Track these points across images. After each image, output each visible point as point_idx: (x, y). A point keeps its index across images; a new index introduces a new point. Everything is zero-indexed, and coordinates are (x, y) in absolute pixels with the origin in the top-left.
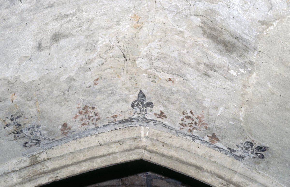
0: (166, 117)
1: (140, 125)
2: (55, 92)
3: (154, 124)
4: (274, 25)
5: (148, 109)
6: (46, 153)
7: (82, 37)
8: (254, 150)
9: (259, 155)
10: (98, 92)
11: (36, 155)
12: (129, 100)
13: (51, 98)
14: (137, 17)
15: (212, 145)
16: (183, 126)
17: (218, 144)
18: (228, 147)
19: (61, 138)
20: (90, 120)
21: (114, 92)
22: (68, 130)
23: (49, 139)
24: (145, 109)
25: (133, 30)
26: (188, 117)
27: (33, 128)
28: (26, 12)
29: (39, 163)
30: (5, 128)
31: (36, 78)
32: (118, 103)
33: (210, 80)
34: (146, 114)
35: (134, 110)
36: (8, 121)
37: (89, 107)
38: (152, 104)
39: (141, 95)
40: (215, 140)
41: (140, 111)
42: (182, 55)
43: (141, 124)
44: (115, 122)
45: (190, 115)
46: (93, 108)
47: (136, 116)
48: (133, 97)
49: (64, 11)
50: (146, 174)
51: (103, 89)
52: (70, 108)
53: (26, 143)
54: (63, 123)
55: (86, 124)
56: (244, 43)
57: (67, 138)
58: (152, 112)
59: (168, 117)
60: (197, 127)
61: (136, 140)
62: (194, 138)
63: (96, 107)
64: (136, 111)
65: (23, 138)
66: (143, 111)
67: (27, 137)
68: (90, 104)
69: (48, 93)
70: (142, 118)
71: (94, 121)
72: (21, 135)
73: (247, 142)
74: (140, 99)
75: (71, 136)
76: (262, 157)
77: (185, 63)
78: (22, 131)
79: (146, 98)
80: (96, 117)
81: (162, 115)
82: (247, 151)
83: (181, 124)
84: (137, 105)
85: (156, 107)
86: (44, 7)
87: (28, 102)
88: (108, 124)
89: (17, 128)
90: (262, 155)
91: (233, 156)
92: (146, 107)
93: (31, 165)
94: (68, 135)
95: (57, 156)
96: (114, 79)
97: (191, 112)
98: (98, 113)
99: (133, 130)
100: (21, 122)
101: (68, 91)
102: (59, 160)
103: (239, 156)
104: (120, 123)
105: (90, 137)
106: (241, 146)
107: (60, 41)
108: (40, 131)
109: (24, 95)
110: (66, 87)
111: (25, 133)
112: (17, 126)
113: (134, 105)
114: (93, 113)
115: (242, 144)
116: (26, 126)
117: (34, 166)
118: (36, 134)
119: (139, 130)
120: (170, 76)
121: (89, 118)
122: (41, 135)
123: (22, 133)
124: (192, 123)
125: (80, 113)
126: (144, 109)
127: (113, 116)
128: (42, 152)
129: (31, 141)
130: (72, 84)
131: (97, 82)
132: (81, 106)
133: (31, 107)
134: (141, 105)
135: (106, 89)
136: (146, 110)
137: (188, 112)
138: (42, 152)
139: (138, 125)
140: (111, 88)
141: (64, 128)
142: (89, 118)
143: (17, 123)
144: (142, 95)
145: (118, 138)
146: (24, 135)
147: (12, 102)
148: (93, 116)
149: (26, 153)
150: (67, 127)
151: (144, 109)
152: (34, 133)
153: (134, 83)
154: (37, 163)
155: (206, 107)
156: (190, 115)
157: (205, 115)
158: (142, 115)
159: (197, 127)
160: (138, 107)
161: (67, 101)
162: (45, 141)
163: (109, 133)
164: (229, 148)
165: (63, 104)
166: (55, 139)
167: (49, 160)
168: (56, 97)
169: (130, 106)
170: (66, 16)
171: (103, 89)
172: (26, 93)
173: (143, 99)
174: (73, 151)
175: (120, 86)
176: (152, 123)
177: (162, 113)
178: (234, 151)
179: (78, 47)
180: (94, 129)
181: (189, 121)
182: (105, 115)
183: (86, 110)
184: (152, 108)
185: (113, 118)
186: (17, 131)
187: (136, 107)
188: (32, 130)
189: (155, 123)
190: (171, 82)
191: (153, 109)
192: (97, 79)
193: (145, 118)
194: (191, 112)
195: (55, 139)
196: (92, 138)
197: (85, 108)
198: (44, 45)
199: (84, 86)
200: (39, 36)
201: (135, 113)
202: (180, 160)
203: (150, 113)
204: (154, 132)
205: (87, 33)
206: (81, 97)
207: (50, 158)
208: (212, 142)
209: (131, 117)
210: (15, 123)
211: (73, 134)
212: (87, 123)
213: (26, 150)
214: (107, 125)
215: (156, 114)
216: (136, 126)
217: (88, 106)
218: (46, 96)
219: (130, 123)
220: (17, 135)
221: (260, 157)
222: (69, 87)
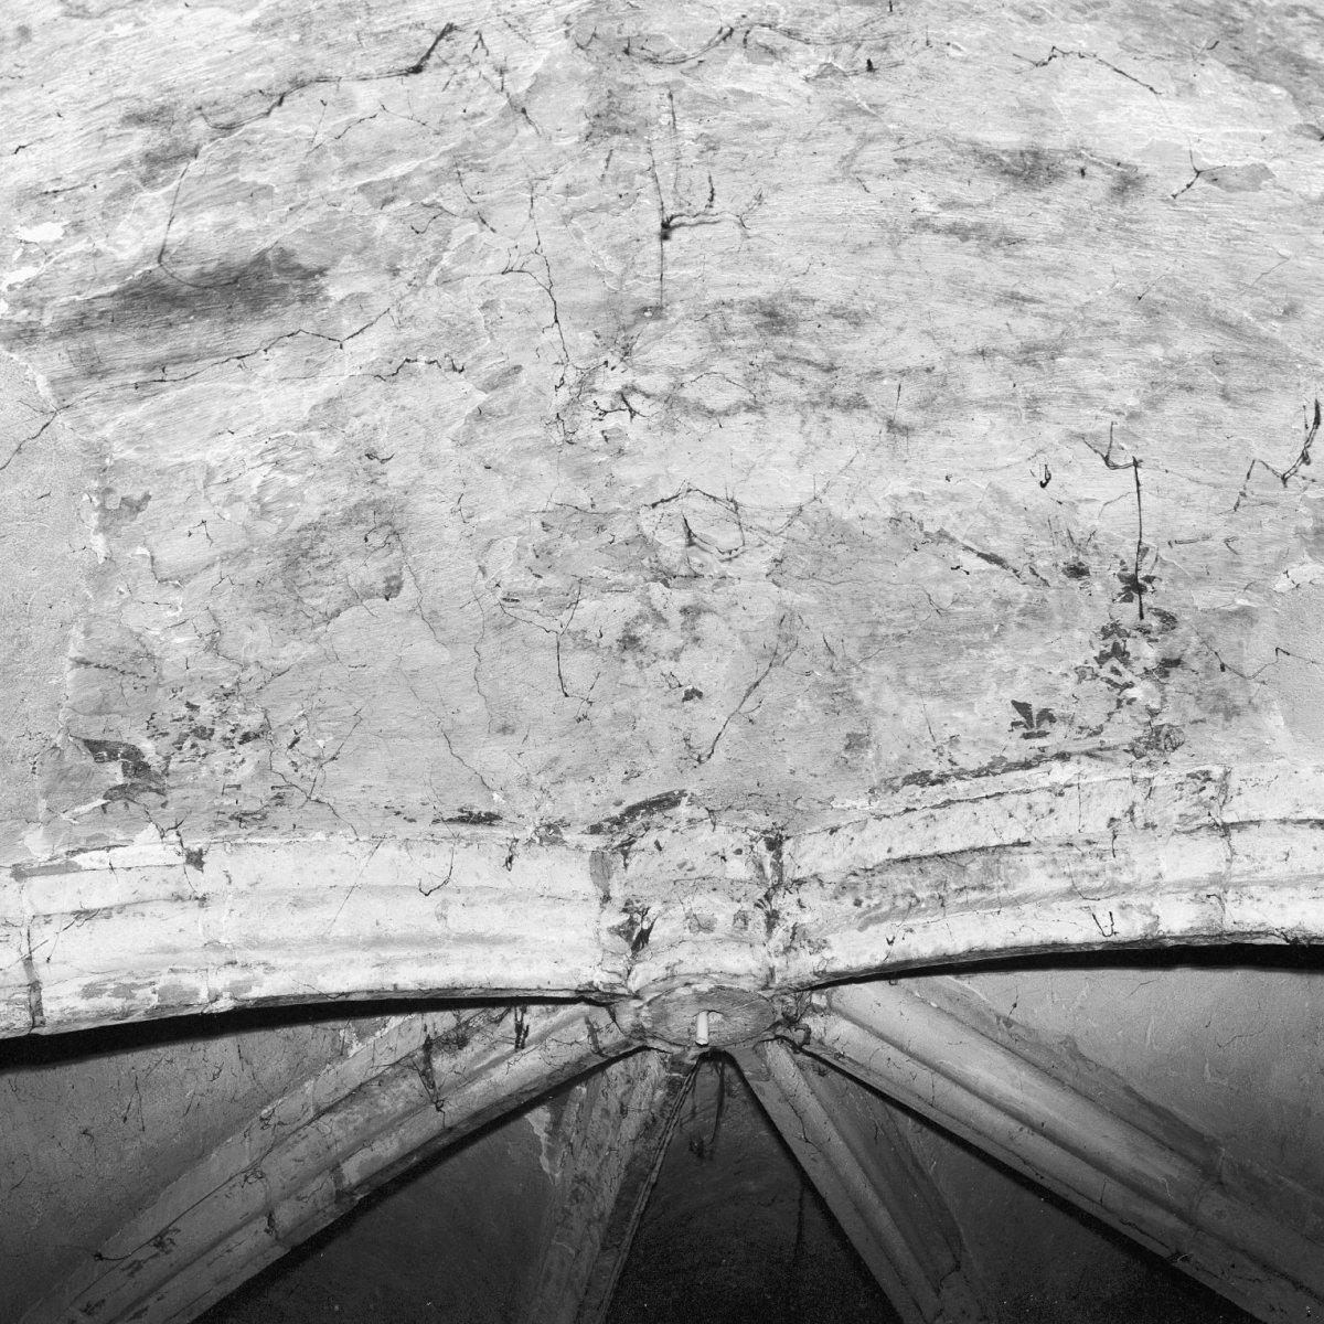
4: (96, 533)
14: (616, 180)
28: (1122, 330)
49: (963, 259)
86: (1042, 309)
170: (959, 232)
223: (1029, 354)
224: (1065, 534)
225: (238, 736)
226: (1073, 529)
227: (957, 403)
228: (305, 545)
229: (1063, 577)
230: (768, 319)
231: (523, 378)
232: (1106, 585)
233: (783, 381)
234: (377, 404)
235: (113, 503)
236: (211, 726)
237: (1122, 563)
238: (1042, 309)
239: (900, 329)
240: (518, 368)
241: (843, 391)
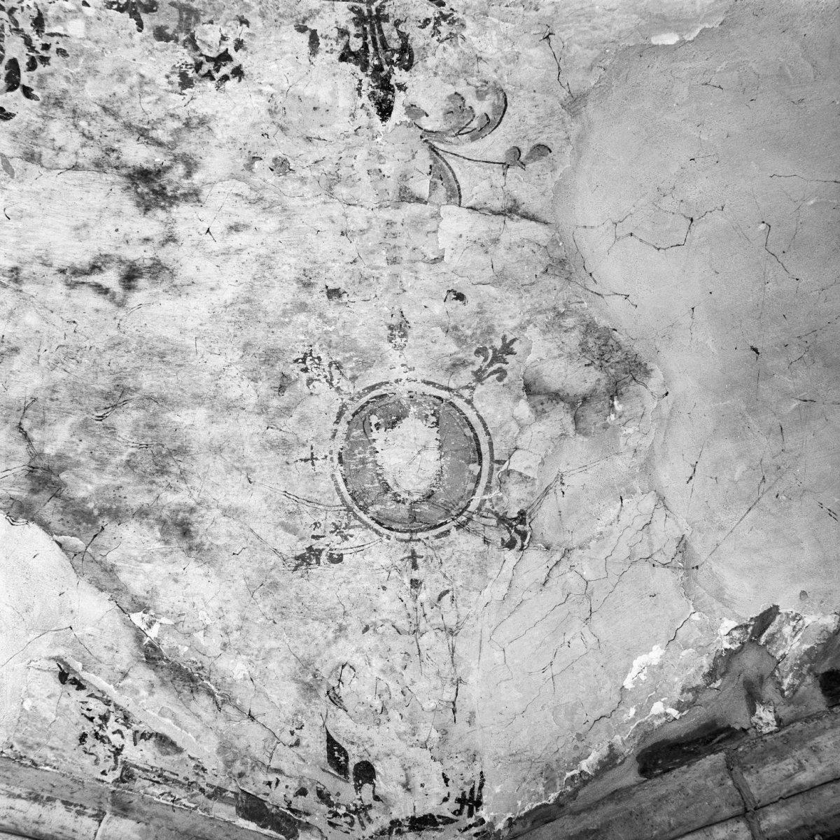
50: (475, 825)
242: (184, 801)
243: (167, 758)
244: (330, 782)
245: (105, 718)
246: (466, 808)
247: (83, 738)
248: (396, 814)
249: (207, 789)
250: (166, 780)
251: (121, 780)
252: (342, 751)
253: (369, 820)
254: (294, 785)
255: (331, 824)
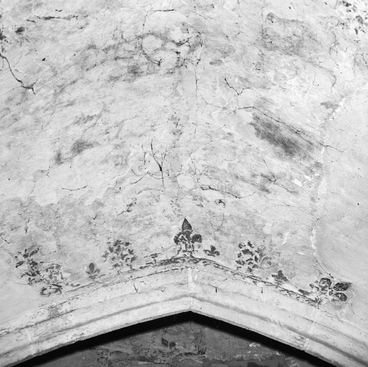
0: (218, 254)
1: (187, 267)
2: (78, 221)
3: (204, 264)
4: (341, 106)
5: (196, 244)
6: (69, 303)
7: (110, 148)
8: (333, 289)
9: (340, 295)
10: (133, 222)
11: (56, 306)
12: (171, 233)
13: (74, 228)
14: (176, 118)
15: (279, 289)
16: (240, 264)
17: (286, 286)
18: (299, 288)
19: (88, 284)
20: (123, 259)
21: (152, 222)
22: (97, 273)
23: (72, 285)
24: (191, 244)
25: (172, 137)
26: (246, 252)
27: (53, 268)
28: (42, 111)
29: (59, 315)
30: (17, 267)
31: (55, 201)
32: (157, 237)
33: (269, 196)
34: (193, 251)
35: (179, 246)
36: (21, 258)
37: (122, 242)
38: (201, 236)
39: (186, 226)
40: (283, 281)
41: (186, 247)
42: (233, 166)
43: (188, 265)
44: (155, 263)
45: (248, 247)
46: (127, 244)
47: (181, 254)
48: (176, 228)
49: (87, 112)
50: (203, 357)
51: (139, 219)
52: (98, 242)
53: (44, 289)
54: (89, 263)
55: (119, 266)
56: (307, 138)
57: (95, 284)
58: (201, 248)
59: (221, 254)
60: (258, 264)
61: (183, 286)
62: (256, 280)
63: (130, 242)
64: (181, 248)
65: (39, 282)
66: (190, 247)
67: (45, 280)
68: (122, 238)
69: (69, 222)
70: (188, 257)
71: (129, 262)
72: (37, 277)
73: (323, 279)
74: (185, 231)
75: (100, 281)
76: (344, 298)
77: (237, 177)
78: (38, 272)
79: (192, 229)
80: (131, 256)
81: (213, 251)
82: (324, 292)
83: (237, 262)
84: (181, 240)
85: (206, 241)
86: (63, 105)
87: (45, 233)
88: (146, 265)
89: (32, 267)
90: (344, 295)
91: (306, 301)
92: (193, 242)
93: (50, 319)
94: (96, 280)
95: (83, 306)
96: (152, 204)
97: (249, 244)
98: (133, 251)
99: (178, 273)
100: (37, 259)
101: (94, 219)
102: (85, 312)
103: (314, 299)
104: (162, 264)
105: (124, 283)
106: (316, 285)
107: (84, 152)
108: (61, 273)
109: (40, 223)
110: (92, 214)
111: (42, 276)
112: (32, 265)
113: (178, 239)
114: (127, 250)
115: (317, 282)
116: (44, 265)
117: (53, 320)
118: (55, 277)
119: (185, 273)
120: (221, 197)
121: (123, 257)
122: (62, 278)
123: (38, 275)
124: (251, 259)
125: (111, 250)
126: (191, 245)
127: (152, 255)
128: (65, 302)
129: (51, 287)
130: (99, 210)
131: (131, 208)
132: (112, 241)
133: (49, 239)
134: (186, 239)
135: (142, 218)
136: (193, 246)
137: (246, 244)
138: (65, 302)
139: (184, 267)
140: (148, 217)
141: (91, 270)
142: (122, 257)
143: (32, 260)
144: (187, 225)
145: (159, 284)
146: (41, 278)
147: (25, 232)
148: (127, 255)
149: (44, 304)
150: (95, 269)
151: (191, 245)
152: (53, 275)
153: (177, 209)
154: (58, 315)
155: (267, 235)
156: (248, 247)
157: (267, 246)
158: (188, 253)
159: (258, 264)
160: (183, 242)
161: (94, 234)
162: (67, 287)
163: (148, 278)
164: (300, 291)
165: (90, 237)
166: (80, 285)
167: (73, 312)
168: (81, 227)
169: (173, 241)
170: (90, 118)
171: (139, 219)
172: (43, 220)
173: (189, 230)
174: (102, 300)
175: (159, 213)
176: (201, 263)
177: (213, 248)
178: (308, 293)
179: (106, 161)
180: (128, 272)
181: (248, 256)
182: (142, 254)
183: (118, 247)
184: (200, 243)
185: (152, 257)
186: (32, 272)
187: (181, 243)
188: (50, 271)
189: (206, 264)
190: (222, 204)
191: (202, 243)
192: (131, 205)
193: (193, 257)
194: (249, 244)
195: (80, 285)
196: (126, 284)
197: (117, 243)
198: (64, 156)
199: (114, 213)
200: (58, 144)
201: (179, 251)
202: (239, 310)
203: (199, 250)
204: (204, 275)
205: (116, 142)
206: (111, 229)
207: (73, 309)
208: (278, 284)
209: (175, 256)
210: (29, 261)
211: (102, 278)
212: (120, 264)
213: (44, 299)
214: (145, 267)
215: (205, 251)
216: (181, 268)
217: (121, 241)
218: (68, 226)
219: (174, 264)
220: (32, 278)
221: (341, 299)
222: (96, 214)
223: (62, 89)
224: (29, 40)
225: (350, 8)
226: (28, 43)
227: (77, 63)
228: (291, 49)
229: (24, 26)
230: (136, 71)
231: (210, 60)
232: (8, 32)
233: (130, 49)
234: (253, 76)
235: (329, 111)
236: (356, 18)
237: (7, 42)
238: (63, 105)
239: (98, 80)
240: (211, 63)
241: (111, 52)
242: (125, 364)
243: (119, 355)
244: (162, 348)
245: (102, 353)
246: (201, 353)
247: (98, 360)
248: (181, 352)
249: (130, 359)
250: (120, 360)
251: (109, 365)
252: (166, 341)
253: (173, 354)
254: (153, 351)
255: (163, 357)
